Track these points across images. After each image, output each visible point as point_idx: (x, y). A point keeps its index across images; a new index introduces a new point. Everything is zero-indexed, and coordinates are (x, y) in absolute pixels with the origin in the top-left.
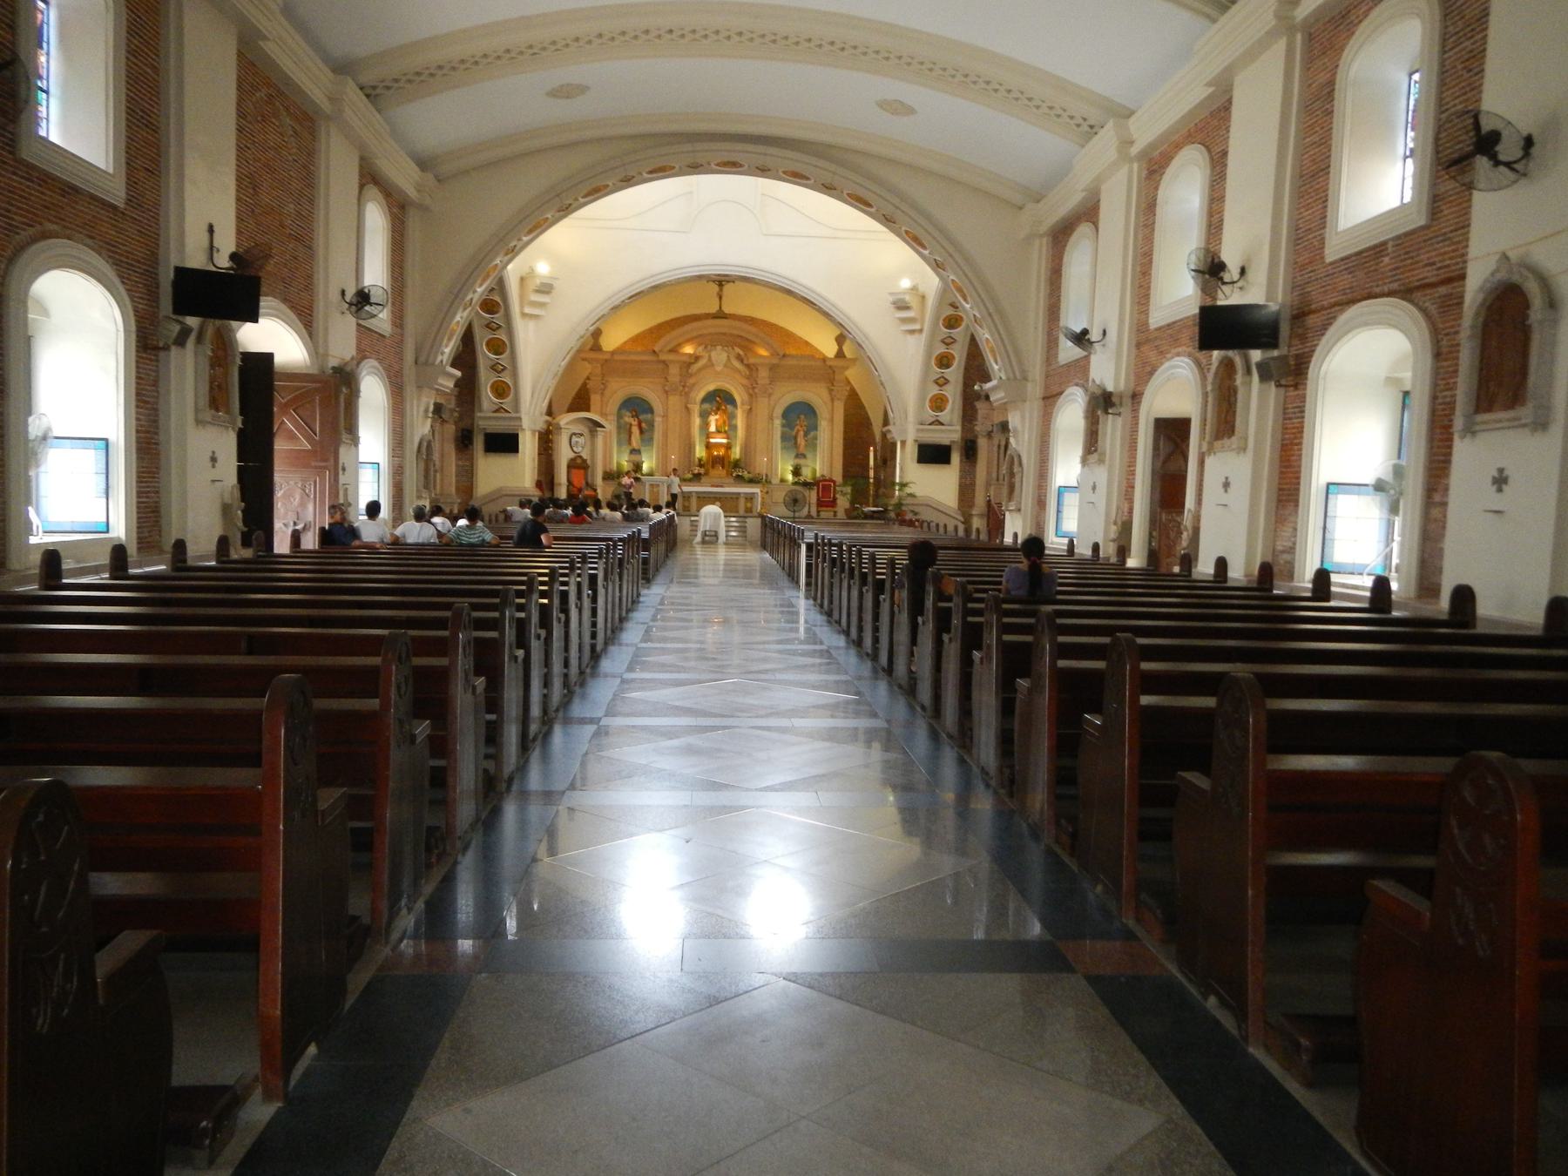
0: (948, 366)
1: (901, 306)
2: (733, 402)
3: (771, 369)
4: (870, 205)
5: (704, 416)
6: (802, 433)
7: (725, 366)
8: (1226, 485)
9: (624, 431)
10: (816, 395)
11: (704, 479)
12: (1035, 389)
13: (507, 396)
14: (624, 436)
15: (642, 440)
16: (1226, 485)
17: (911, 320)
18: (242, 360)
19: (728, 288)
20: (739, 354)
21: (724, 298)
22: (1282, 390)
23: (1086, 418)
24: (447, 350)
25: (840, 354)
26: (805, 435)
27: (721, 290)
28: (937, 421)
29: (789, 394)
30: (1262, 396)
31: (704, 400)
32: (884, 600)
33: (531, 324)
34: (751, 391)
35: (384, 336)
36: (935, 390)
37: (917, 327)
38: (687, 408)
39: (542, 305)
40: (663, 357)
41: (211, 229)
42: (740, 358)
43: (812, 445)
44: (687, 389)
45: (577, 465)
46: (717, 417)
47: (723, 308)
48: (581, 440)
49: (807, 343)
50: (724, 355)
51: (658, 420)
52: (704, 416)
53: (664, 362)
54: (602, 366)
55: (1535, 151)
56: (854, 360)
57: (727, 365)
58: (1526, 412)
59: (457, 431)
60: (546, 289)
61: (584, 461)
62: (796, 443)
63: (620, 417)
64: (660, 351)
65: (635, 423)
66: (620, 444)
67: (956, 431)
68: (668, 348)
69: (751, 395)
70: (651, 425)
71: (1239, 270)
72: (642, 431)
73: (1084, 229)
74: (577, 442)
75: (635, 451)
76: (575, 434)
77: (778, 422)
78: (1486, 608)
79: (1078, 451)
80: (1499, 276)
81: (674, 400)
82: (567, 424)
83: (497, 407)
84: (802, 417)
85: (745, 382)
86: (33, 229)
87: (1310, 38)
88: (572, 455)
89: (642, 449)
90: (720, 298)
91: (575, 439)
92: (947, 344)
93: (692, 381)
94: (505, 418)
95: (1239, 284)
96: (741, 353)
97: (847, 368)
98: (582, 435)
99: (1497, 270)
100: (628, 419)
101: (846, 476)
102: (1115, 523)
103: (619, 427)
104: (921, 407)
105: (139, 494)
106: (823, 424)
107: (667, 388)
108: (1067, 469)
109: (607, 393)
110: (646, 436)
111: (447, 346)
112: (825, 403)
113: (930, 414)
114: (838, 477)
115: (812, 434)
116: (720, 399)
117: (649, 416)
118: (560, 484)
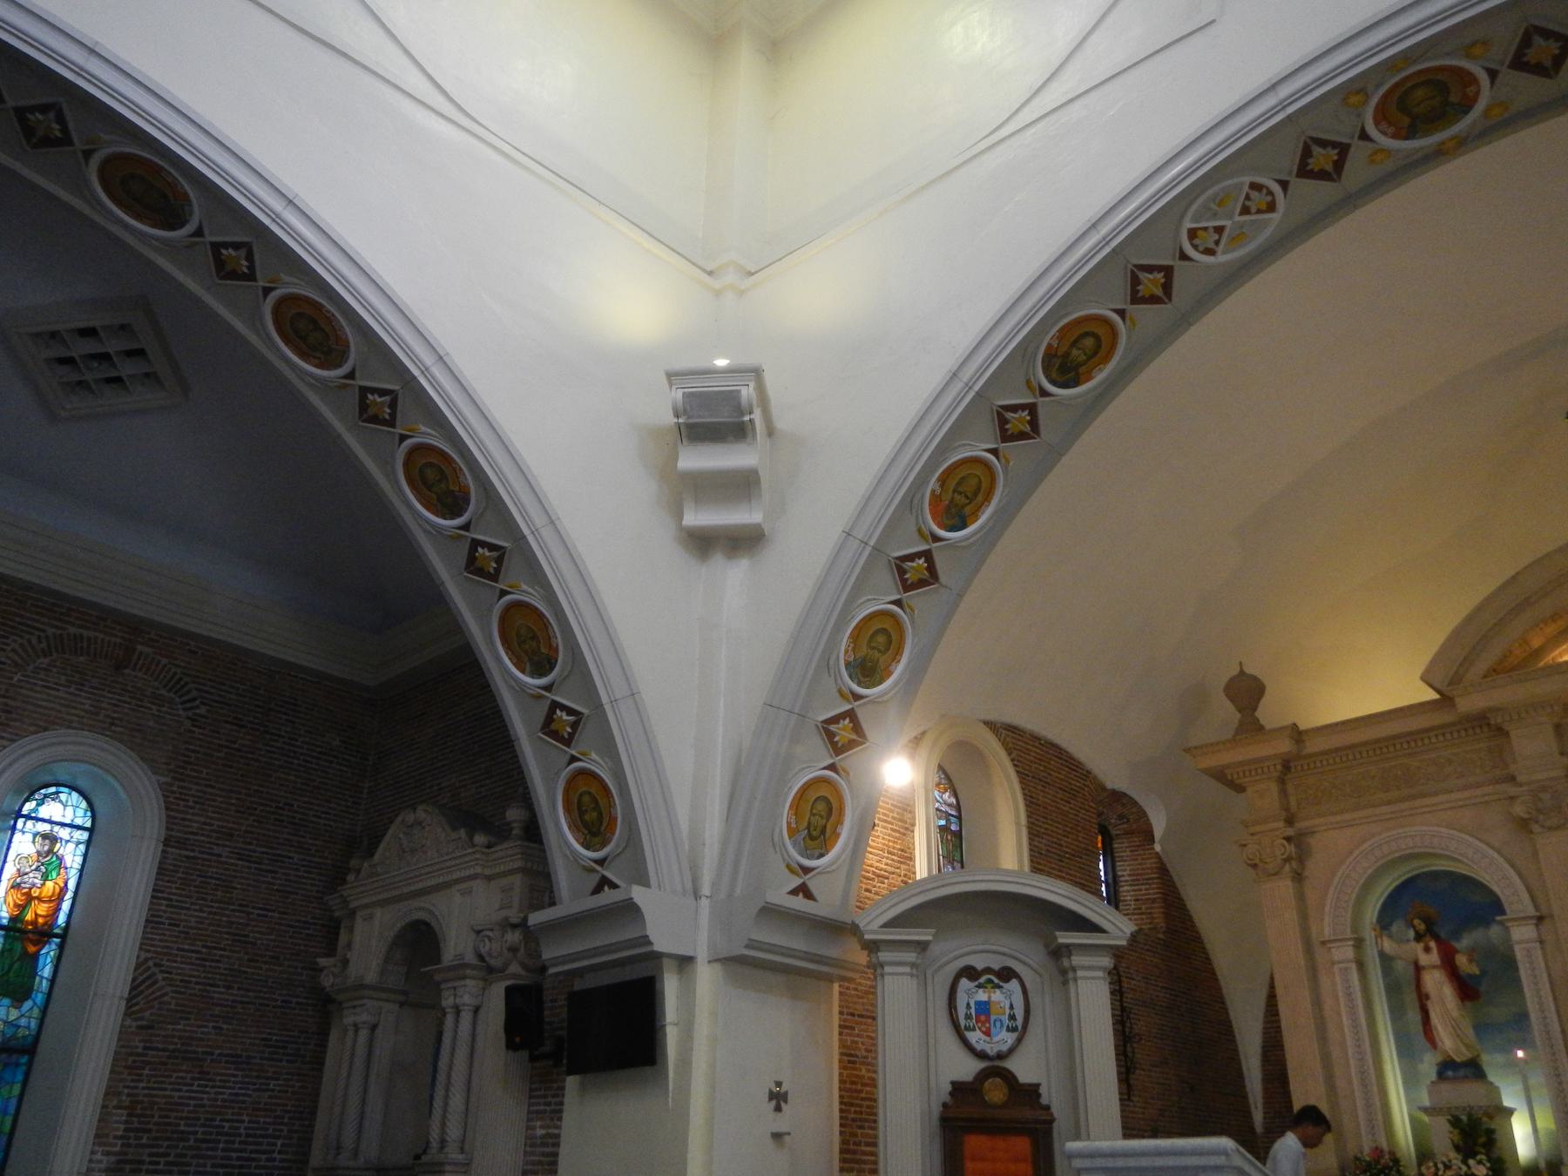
14: (1414, 1016)
15: (1481, 1028)
33: (734, 575)
39: (743, 485)
40: (1469, 703)
48: (1004, 998)
51: (1522, 934)
53: (1488, 726)
54: (1282, 781)
64: (1456, 680)
65: (1431, 958)
66: (1406, 1052)
68: (1482, 666)
70: (1503, 965)
72: (1467, 990)
74: (984, 1009)
76: (970, 973)
88: (966, 1068)
89: (1492, 1063)
98: (1006, 974)
103: (1393, 989)
107: (1519, 810)
109: (1314, 868)
117: (1494, 932)
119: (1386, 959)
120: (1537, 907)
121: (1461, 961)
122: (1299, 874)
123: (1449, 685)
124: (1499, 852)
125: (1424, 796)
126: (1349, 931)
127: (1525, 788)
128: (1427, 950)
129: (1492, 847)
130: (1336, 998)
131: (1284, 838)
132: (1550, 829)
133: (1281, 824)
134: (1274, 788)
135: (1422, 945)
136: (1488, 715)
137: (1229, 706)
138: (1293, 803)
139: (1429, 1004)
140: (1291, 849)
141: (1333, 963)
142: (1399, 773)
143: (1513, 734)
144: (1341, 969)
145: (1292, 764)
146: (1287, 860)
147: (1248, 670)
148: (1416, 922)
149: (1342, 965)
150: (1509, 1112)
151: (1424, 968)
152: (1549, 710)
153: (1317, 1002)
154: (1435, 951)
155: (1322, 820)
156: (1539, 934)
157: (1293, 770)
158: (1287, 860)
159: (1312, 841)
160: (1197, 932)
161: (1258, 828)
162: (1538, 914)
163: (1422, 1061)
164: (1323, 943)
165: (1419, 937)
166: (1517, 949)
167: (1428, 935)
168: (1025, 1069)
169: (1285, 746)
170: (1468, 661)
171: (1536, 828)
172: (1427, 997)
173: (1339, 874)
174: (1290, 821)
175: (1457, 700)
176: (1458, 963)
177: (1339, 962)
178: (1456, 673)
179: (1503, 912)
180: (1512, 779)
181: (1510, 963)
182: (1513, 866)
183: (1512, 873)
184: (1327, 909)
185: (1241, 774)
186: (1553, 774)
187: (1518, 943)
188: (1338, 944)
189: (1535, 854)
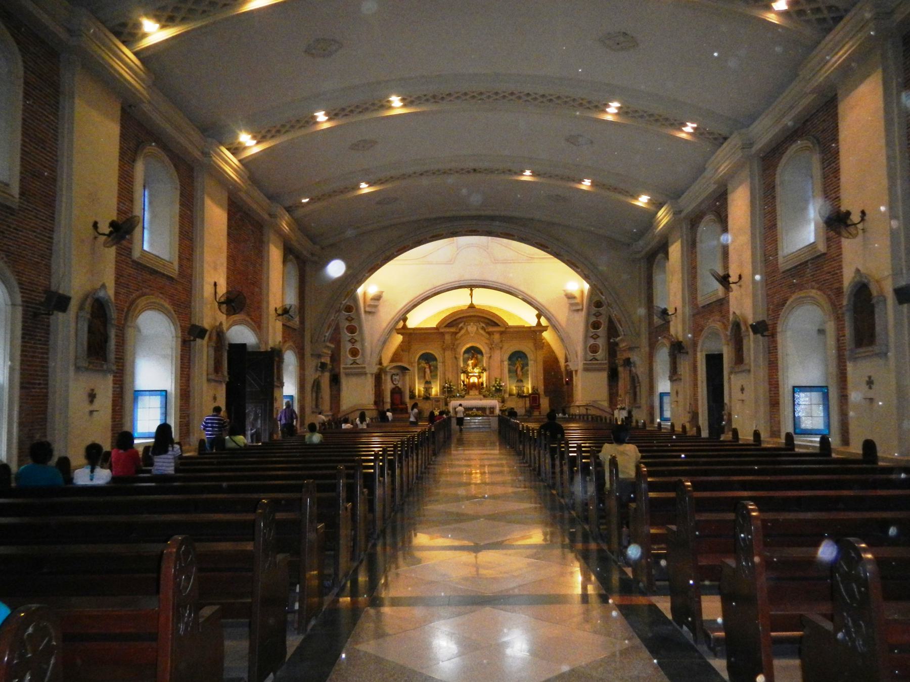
0: (598, 328)
1: (570, 297)
2: (481, 353)
4: (547, 247)
5: (465, 361)
6: (519, 369)
7: (476, 333)
8: (742, 390)
9: (422, 372)
10: (526, 347)
11: (466, 397)
12: (644, 341)
13: (358, 355)
14: (422, 374)
15: (431, 376)
16: (742, 390)
17: (577, 304)
18: (229, 347)
22: (766, 338)
23: (670, 355)
24: (327, 334)
25: (539, 324)
26: (522, 369)
27: (472, 292)
28: (594, 358)
29: (513, 346)
30: (755, 342)
31: (466, 352)
32: (557, 457)
33: (370, 317)
34: (490, 346)
35: (295, 329)
36: (592, 342)
37: (580, 307)
38: (456, 358)
40: (442, 330)
41: (215, 284)
42: (483, 328)
43: (525, 374)
44: (455, 347)
45: (397, 392)
46: (472, 361)
48: (397, 377)
49: (520, 319)
51: (440, 365)
52: (465, 361)
55: (866, 218)
56: (547, 327)
57: (477, 333)
58: (876, 349)
59: (331, 375)
60: (378, 298)
61: (400, 389)
62: (517, 374)
63: (419, 364)
65: (427, 366)
67: (606, 364)
69: (491, 349)
70: (436, 368)
71: (738, 277)
72: (431, 372)
73: (660, 256)
75: (428, 383)
76: (394, 374)
77: (506, 363)
78: (881, 451)
79: (667, 374)
80: (856, 280)
81: (448, 354)
82: (391, 369)
83: (352, 362)
84: (519, 359)
85: (487, 341)
86: (138, 293)
87: (763, 159)
88: (394, 386)
89: (432, 381)
90: (472, 297)
91: (394, 377)
92: (597, 316)
93: (458, 342)
94: (355, 368)
95: (738, 284)
96: (484, 325)
97: (543, 331)
98: (397, 374)
99: (855, 277)
100: (423, 364)
101: (547, 392)
102: (689, 413)
103: (419, 369)
104: (586, 353)
105: (181, 417)
106: (531, 363)
108: (664, 385)
110: (433, 374)
111: (327, 332)
112: (532, 351)
113: (590, 355)
114: (541, 390)
115: (526, 368)
116: (474, 352)
117: (435, 362)
118: (387, 402)
168: (399, 385)
180: (444, 342)
189: (444, 353)
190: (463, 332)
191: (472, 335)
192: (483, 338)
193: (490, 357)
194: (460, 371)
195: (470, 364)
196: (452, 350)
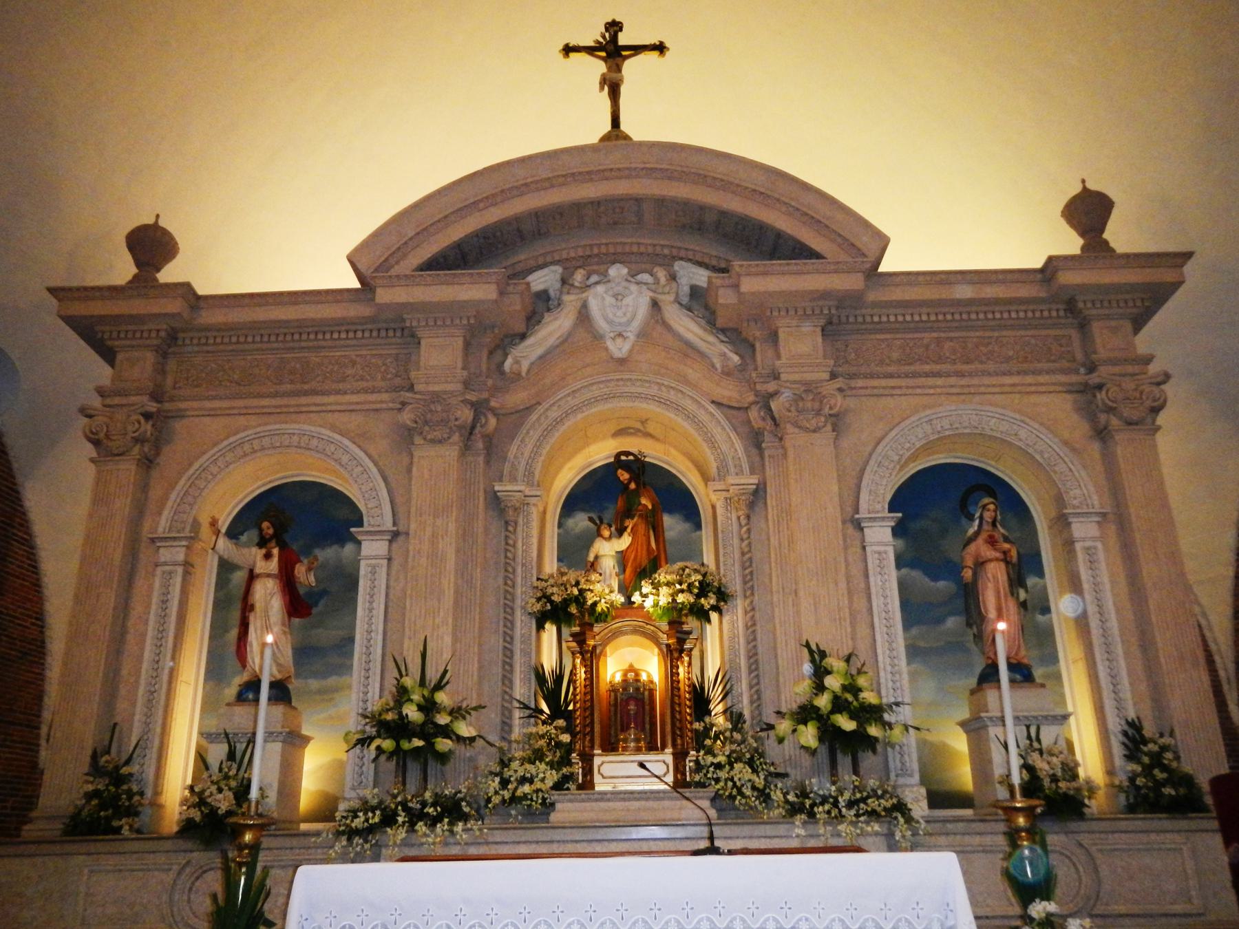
3: (830, 330)
6: (996, 574)
7: (643, 334)
14: (234, 633)
19: (632, 68)
20: (695, 292)
21: (624, 90)
26: (1017, 580)
31: (574, 502)
38: (496, 502)
42: (698, 300)
44: (493, 421)
46: (625, 542)
47: (624, 127)
50: (637, 302)
51: (372, 549)
54: (163, 354)
64: (384, 266)
66: (215, 672)
69: (755, 440)
85: (729, 391)
93: (516, 398)
96: (701, 277)
103: (221, 604)
107: (406, 417)
109: (170, 457)
117: (349, 548)
119: (226, 567)
120: (395, 524)
121: (300, 571)
122: (151, 461)
123: (376, 270)
124: (376, 464)
125: (315, 392)
126: (188, 528)
127: (418, 396)
128: (268, 556)
129: (370, 457)
130: (148, 606)
131: (142, 414)
132: (433, 441)
133: (145, 399)
134: (150, 357)
135: (264, 551)
136: (405, 316)
137: (128, 257)
138: (169, 381)
139: (252, 618)
140: (147, 427)
141: (157, 566)
142: (298, 366)
143: (423, 342)
144: (164, 572)
145: (181, 335)
146: (136, 440)
147: (162, 223)
148: (265, 525)
149: (167, 568)
150: (307, 740)
151: (259, 576)
152: (465, 322)
153: (124, 607)
154: (276, 559)
155: (195, 404)
156: (390, 551)
157: (180, 342)
158: (136, 440)
159: (179, 425)
160: (30, 535)
161: (117, 400)
162: (395, 529)
163: (229, 685)
164: (153, 540)
165: (262, 543)
166: (363, 563)
167: (274, 541)
169: (173, 306)
170: (401, 251)
171: (418, 440)
172: (252, 608)
173: (196, 465)
174: (157, 396)
175: (379, 291)
176: (296, 571)
177: (165, 564)
178: (386, 260)
179: (360, 523)
180: (411, 388)
181: (352, 583)
182: (385, 479)
183: (382, 485)
184: (170, 503)
185: (115, 335)
186: (450, 387)
187: (368, 558)
188: (167, 544)
189: (409, 471)
190: (555, 327)
191: (619, 348)
192: (693, 372)
193: (757, 496)
194: (525, 600)
195: (609, 564)
196: (466, 448)
